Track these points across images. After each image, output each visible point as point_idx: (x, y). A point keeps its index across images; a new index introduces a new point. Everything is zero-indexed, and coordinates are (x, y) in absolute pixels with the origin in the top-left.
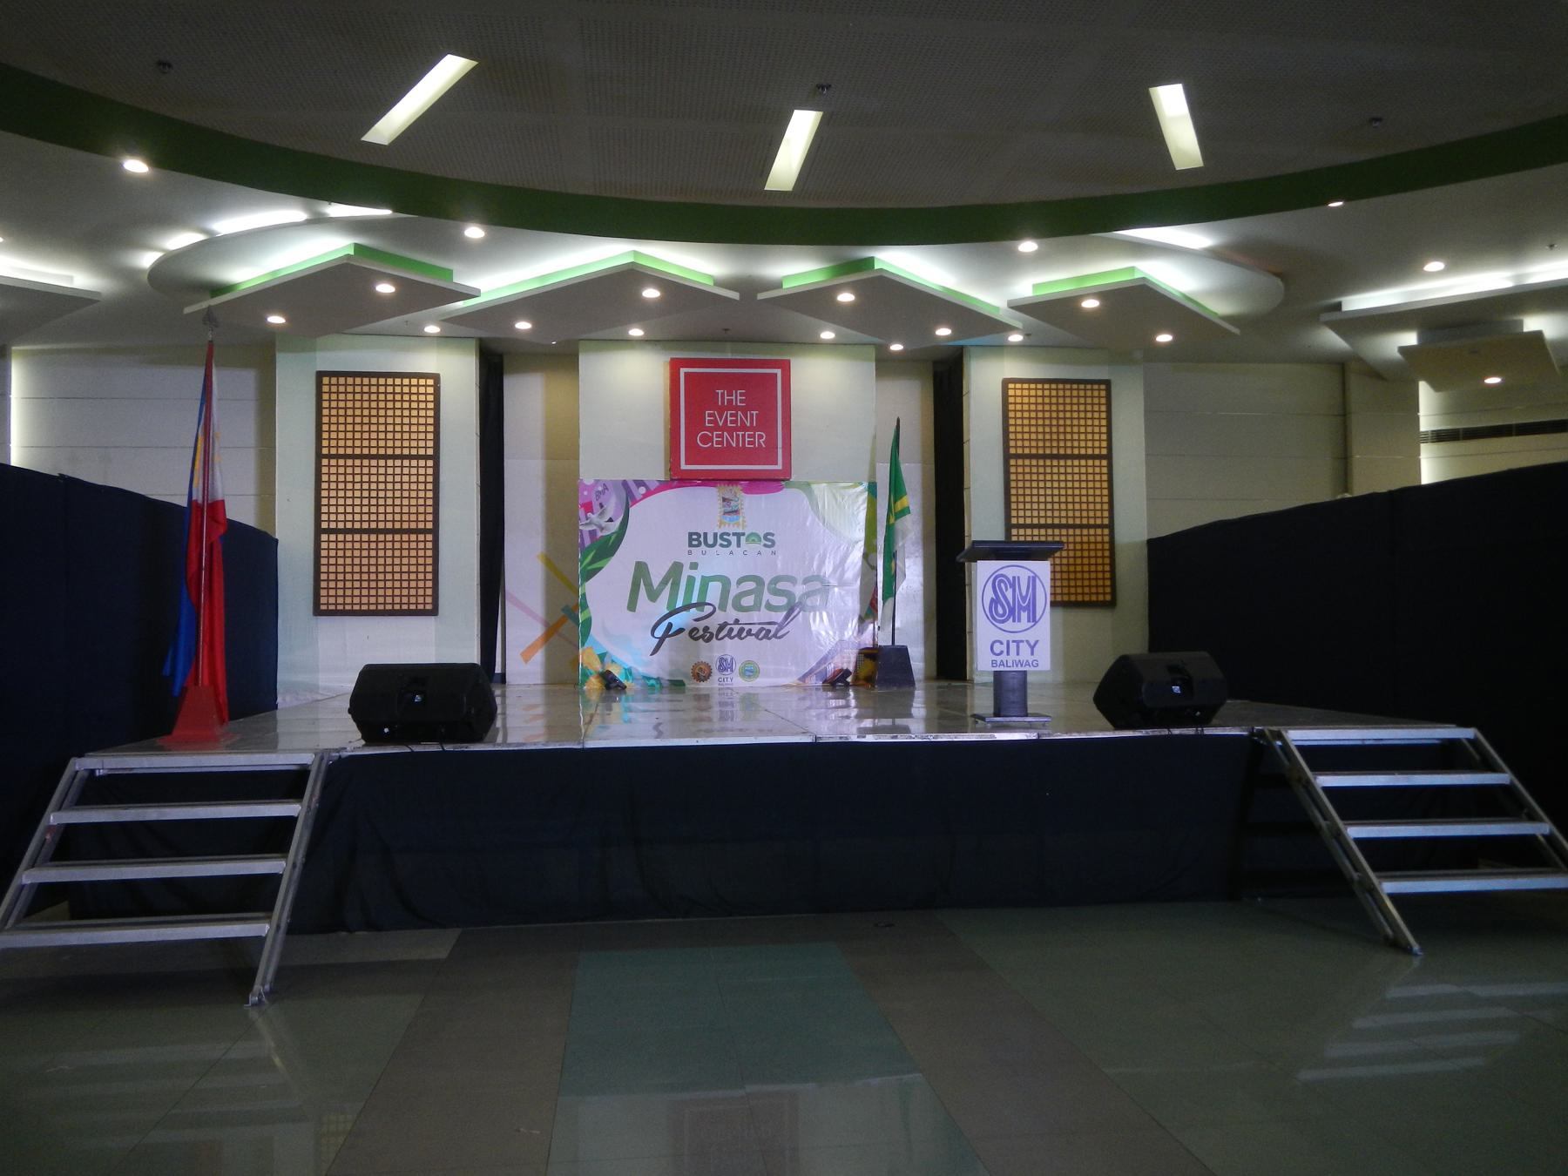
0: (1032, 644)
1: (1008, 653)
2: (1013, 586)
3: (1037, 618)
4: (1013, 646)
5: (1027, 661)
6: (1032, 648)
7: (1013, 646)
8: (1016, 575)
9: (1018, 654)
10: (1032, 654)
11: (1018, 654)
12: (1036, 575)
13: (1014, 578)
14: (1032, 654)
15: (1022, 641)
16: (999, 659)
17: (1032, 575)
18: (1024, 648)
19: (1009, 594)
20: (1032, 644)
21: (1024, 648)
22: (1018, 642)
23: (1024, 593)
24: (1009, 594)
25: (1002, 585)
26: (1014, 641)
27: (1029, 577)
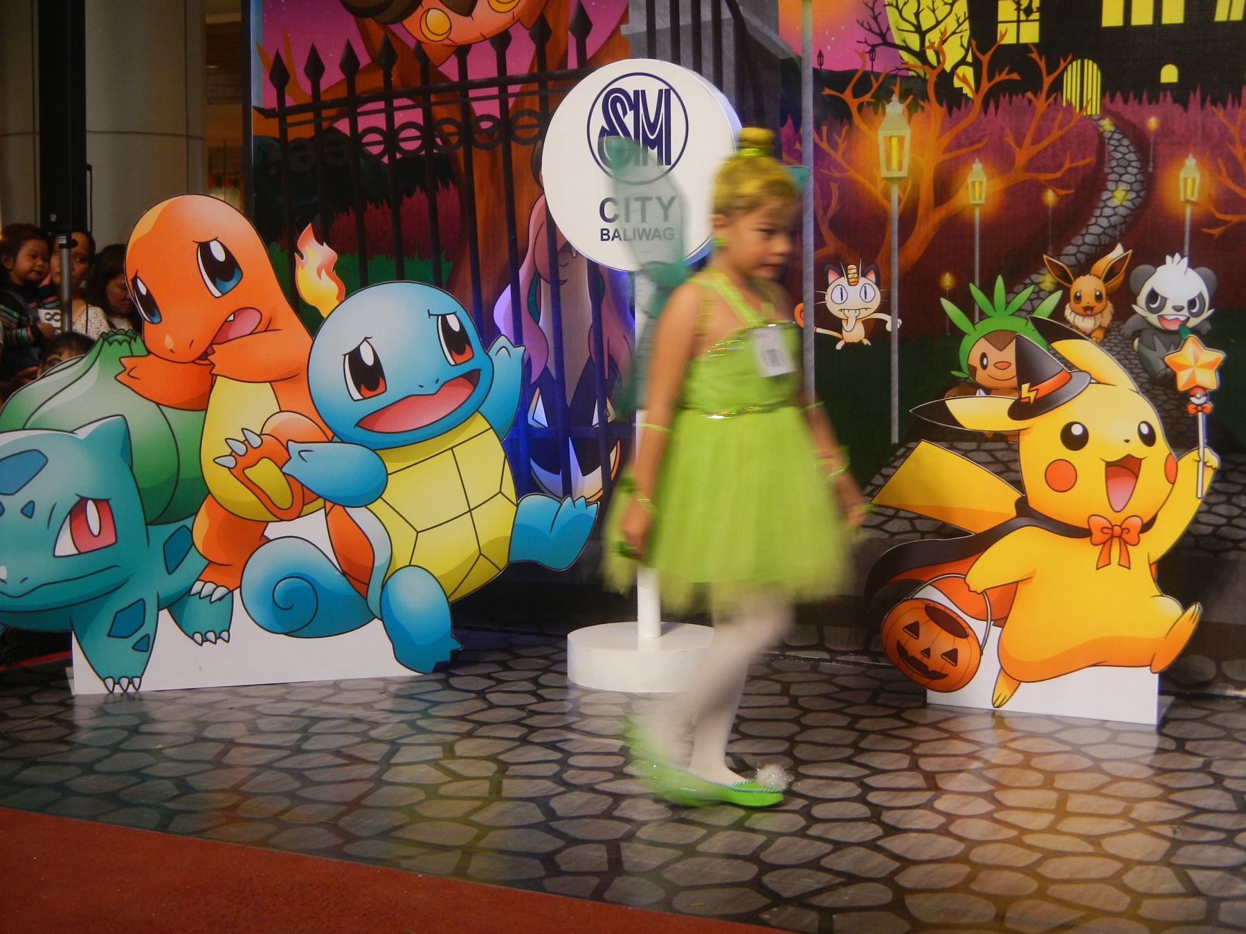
0: (666, 203)
1: (627, 219)
2: (635, 107)
3: (672, 163)
4: (636, 206)
5: (656, 230)
6: (666, 208)
7: (636, 206)
8: (640, 89)
9: (643, 219)
10: (666, 218)
11: (643, 219)
12: (671, 88)
13: (636, 93)
14: (666, 218)
15: (649, 199)
16: (611, 227)
17: (665, 87)
18: (654, 209)
19: (629, 120)
20: (666, 203)
21: (654, 209)
22: (644, 200)
23: (652, 119)
24: (629, 120)
25: (619, 105)
26: (637, 199)
27: (661, 91)
